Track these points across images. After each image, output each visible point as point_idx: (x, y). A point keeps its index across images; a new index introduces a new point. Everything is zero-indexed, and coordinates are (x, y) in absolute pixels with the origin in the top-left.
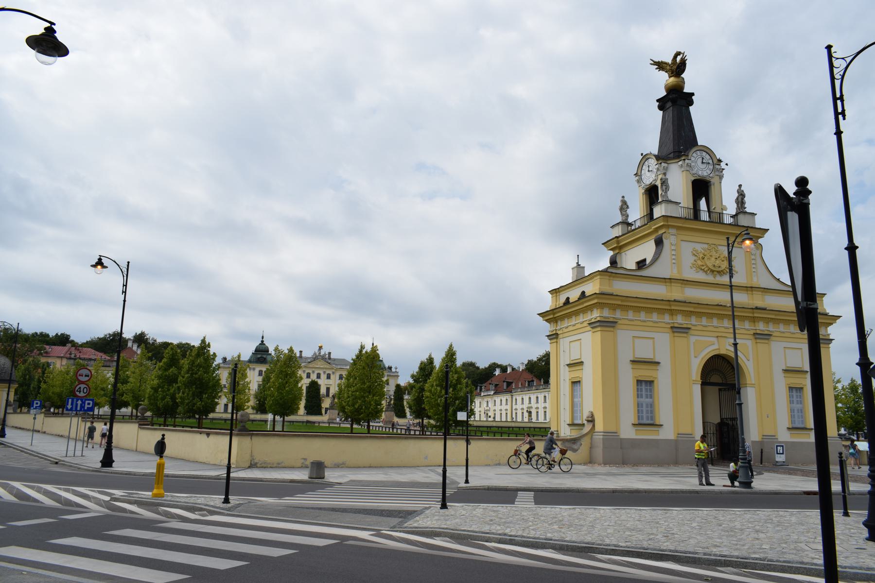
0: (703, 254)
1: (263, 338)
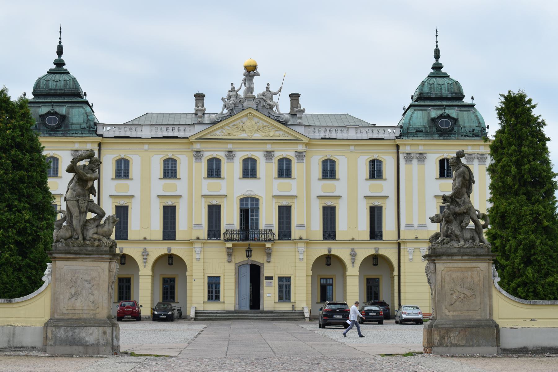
1: (60, 51)
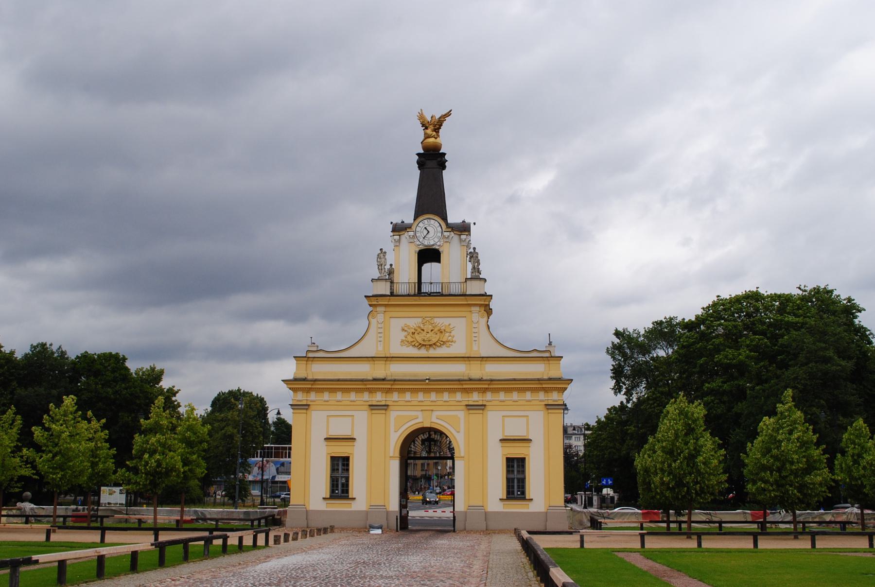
0: (415, 329)
